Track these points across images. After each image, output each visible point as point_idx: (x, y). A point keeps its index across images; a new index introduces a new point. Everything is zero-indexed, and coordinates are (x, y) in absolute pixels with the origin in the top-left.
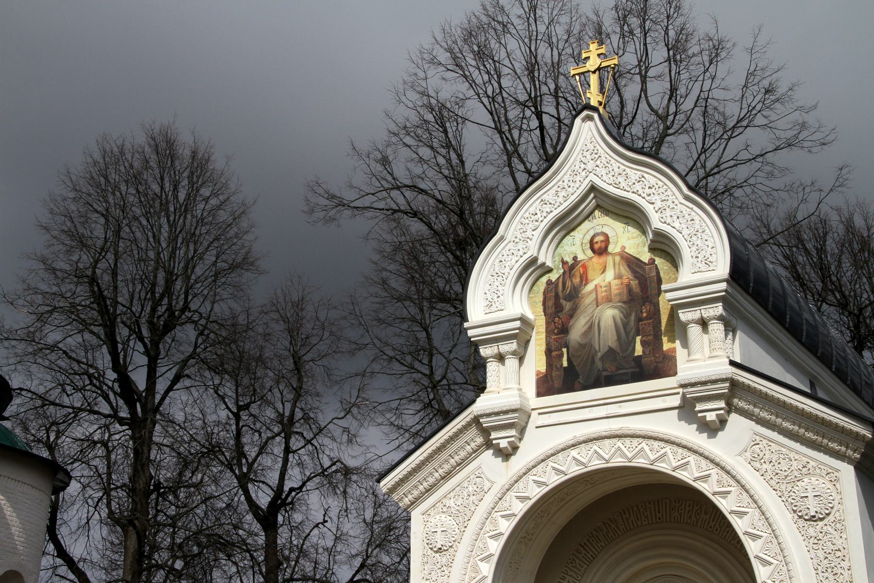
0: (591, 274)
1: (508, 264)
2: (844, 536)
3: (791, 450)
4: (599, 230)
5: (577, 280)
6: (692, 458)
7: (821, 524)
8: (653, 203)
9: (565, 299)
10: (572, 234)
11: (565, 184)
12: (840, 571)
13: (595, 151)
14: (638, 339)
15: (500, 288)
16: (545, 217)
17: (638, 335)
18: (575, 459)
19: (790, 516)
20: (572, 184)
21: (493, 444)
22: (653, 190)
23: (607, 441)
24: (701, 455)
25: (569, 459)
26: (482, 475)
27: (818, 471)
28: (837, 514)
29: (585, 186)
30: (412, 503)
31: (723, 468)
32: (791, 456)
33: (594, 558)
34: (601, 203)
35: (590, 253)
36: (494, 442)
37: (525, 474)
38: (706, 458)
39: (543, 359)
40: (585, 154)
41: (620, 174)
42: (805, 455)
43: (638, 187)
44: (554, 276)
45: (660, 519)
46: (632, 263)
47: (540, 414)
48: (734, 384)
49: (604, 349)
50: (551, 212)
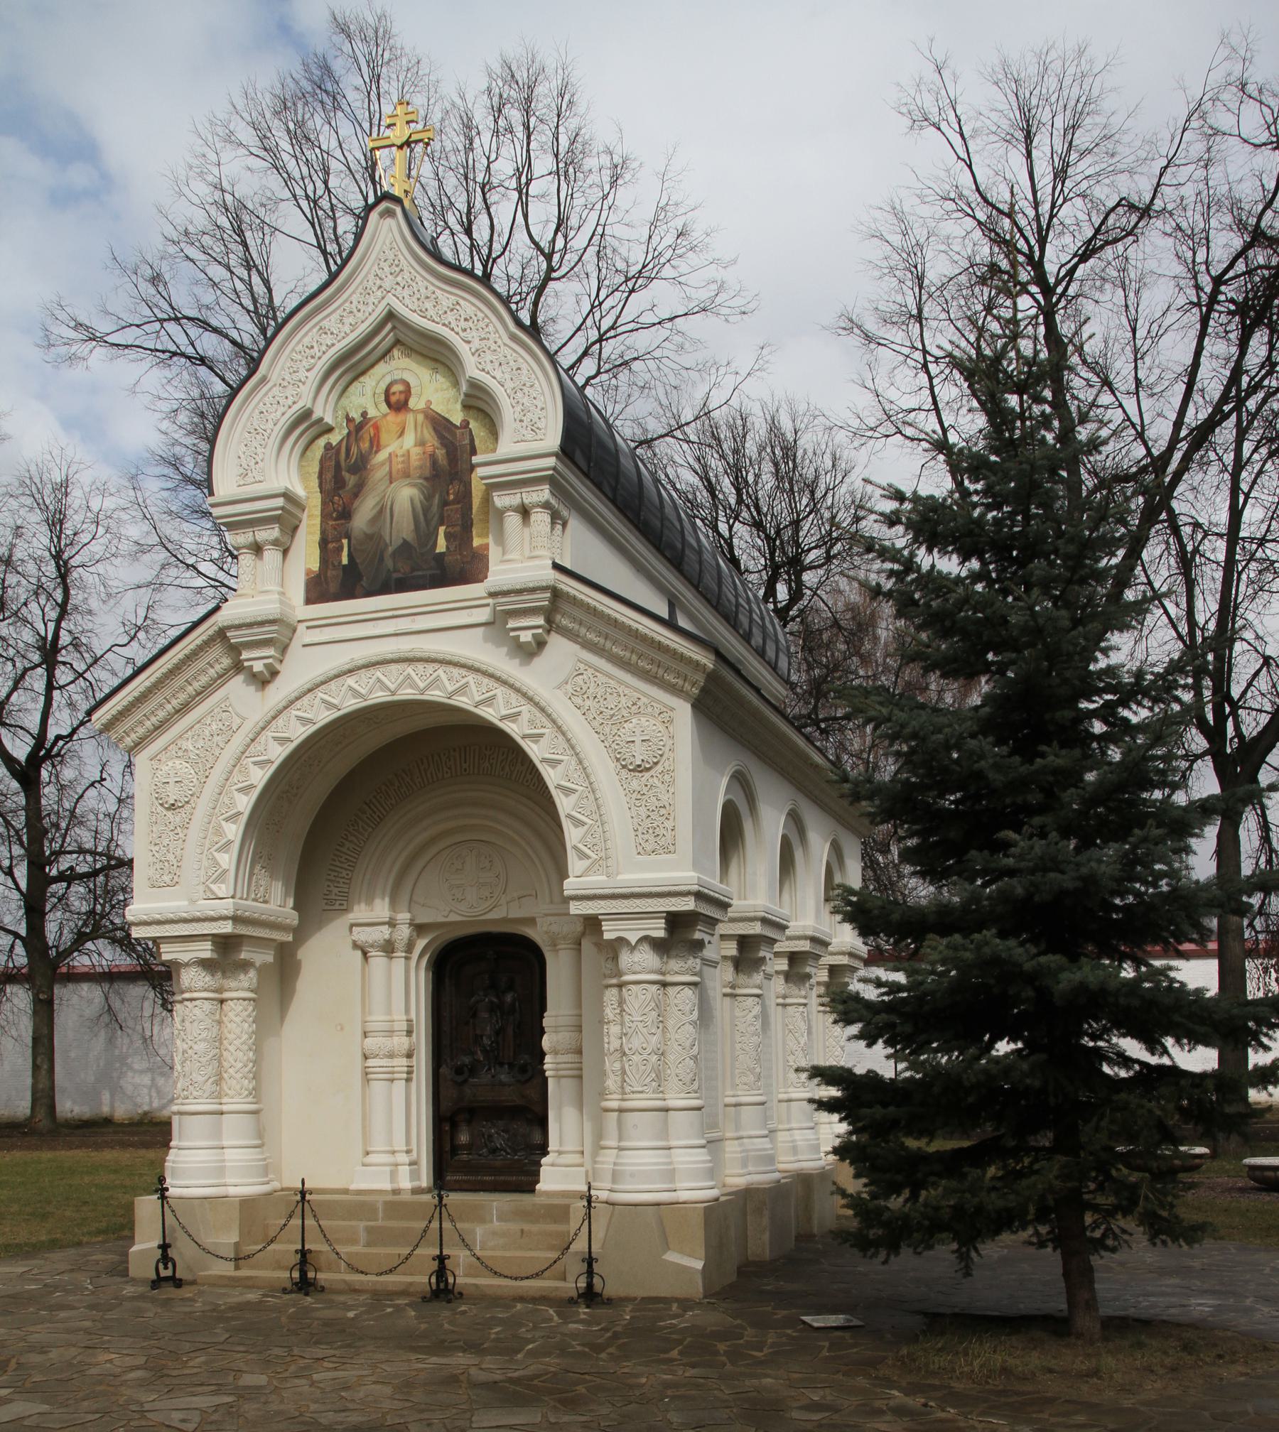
0: (384, 437)
2: (671, 790)
3: (620, 682)
4: (398, 375)
5: (365, 445)
7: (647, 775)
8: (469, 342)
9: (348, 471)
10: (362, 379)
11: (353, 306)
14: (442, 530)
15: (260, 450)
17: (442, 524)
18: (351, 688)
19: (612, 765)
20: (361, 307)
21: (244, 668)
22: (470, 323)
23: (394, 667)
24: (512, 686)
25: (344, 689)
27: (650, 709)
28: (666, 764)
29: (379, 312)
30: (137, 745)
31: (537, 705)
32: (620, 690)
34: (402, 337)
35: (384, 407)
36: (246, 664)
37: (285, 708)
38: (518, 690)
39: (317, 552)
42: (637, 690)
43: (450, 317)
44: (335, 438)
46: (439, 424)
47: (308, 628)
48: (556, 593)
49: (397, 543)
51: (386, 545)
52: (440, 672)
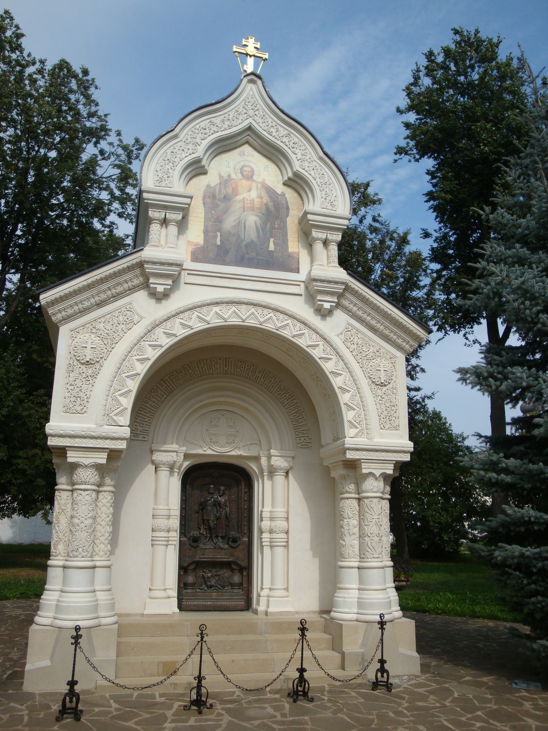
1: (179, 156)
6: (306, 331)
8: (296, 154)
11: (231, 117)
12: (393, 419)
13: (255, 105)
14: (272, 240)
15: (170, 171)
16: (212, 134)
18: (217, 313)
22: (296, 145)
24: (315, 330)
25: (212, 313)
29: (245, 124)
33: (173, 391)
36: (152, 286)
37: (173, 316)
40: (247, 103)
41: (272, 126)
43: (285, 139)
45: (226, 371)
47: (188, 274)
50: (218, 132)
51: (242, 241)
52: (272, 314)
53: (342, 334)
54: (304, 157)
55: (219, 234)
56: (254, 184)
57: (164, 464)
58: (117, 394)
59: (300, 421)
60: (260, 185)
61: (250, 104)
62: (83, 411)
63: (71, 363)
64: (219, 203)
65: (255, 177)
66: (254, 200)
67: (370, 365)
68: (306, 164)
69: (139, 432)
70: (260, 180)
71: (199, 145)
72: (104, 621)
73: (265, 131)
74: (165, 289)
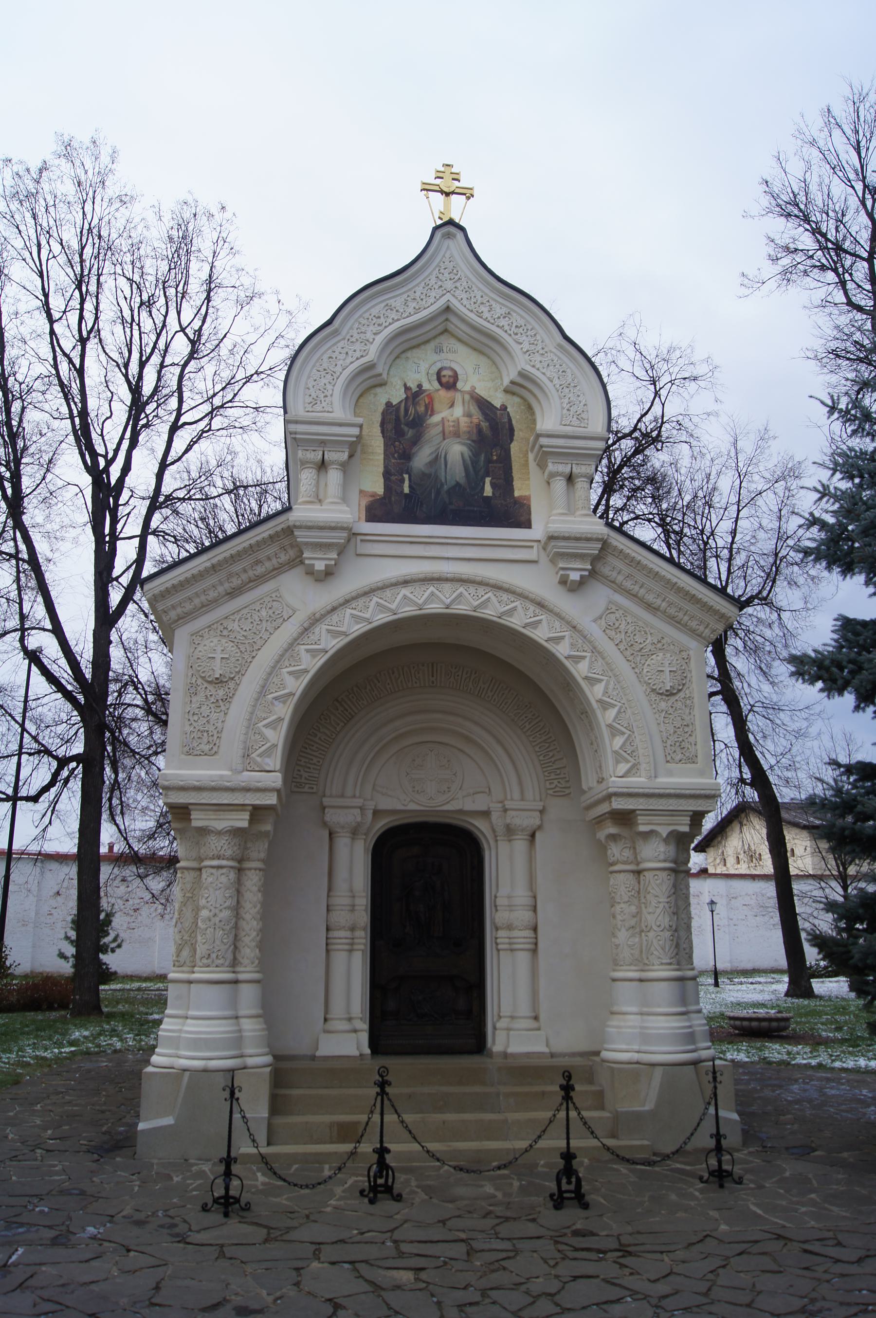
1: (341, 362)
7: (673, 699)
11: (418, 294)
13: (455, 271)
14: (488, 480)
15: (329, 387)
16: (390, 324)
17: (488, 476)
18: (405, 597)
22: (521, 329)
24: (558, 616)
26: (280, 599)
29: (441, 303)
33: (353, 717)
36: (307, 562)
37: (341, 605)
40: (442, 271)
41: (482, 303)
43: (503, 322)
45: (433, 682)
47: (362, 541)
50: (398, 320)
51: (442, 485)
52: (490, 594)
53: (601, 618)
54: (533, 347)
55: (406, 476)
56: (458, 396)
57: (343, 827)
58: (261, 724)
59: (551, 754)
60: (467, 397)
61: (446, 272)
62: (213, 752)
63: (193, 681)
64: (406, 429)
65: (459, 385)
66: (458, 419)
67: (647, 663)
68: (538, 358)
69: (303, 780)
70: (467, 388)
71: (372, 343)
72: (251, 1061)
73: (472, 311)
74: (326, 566)
